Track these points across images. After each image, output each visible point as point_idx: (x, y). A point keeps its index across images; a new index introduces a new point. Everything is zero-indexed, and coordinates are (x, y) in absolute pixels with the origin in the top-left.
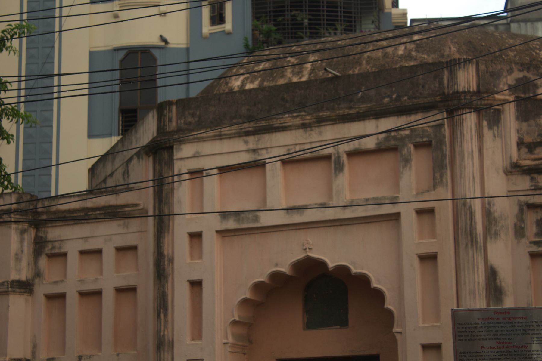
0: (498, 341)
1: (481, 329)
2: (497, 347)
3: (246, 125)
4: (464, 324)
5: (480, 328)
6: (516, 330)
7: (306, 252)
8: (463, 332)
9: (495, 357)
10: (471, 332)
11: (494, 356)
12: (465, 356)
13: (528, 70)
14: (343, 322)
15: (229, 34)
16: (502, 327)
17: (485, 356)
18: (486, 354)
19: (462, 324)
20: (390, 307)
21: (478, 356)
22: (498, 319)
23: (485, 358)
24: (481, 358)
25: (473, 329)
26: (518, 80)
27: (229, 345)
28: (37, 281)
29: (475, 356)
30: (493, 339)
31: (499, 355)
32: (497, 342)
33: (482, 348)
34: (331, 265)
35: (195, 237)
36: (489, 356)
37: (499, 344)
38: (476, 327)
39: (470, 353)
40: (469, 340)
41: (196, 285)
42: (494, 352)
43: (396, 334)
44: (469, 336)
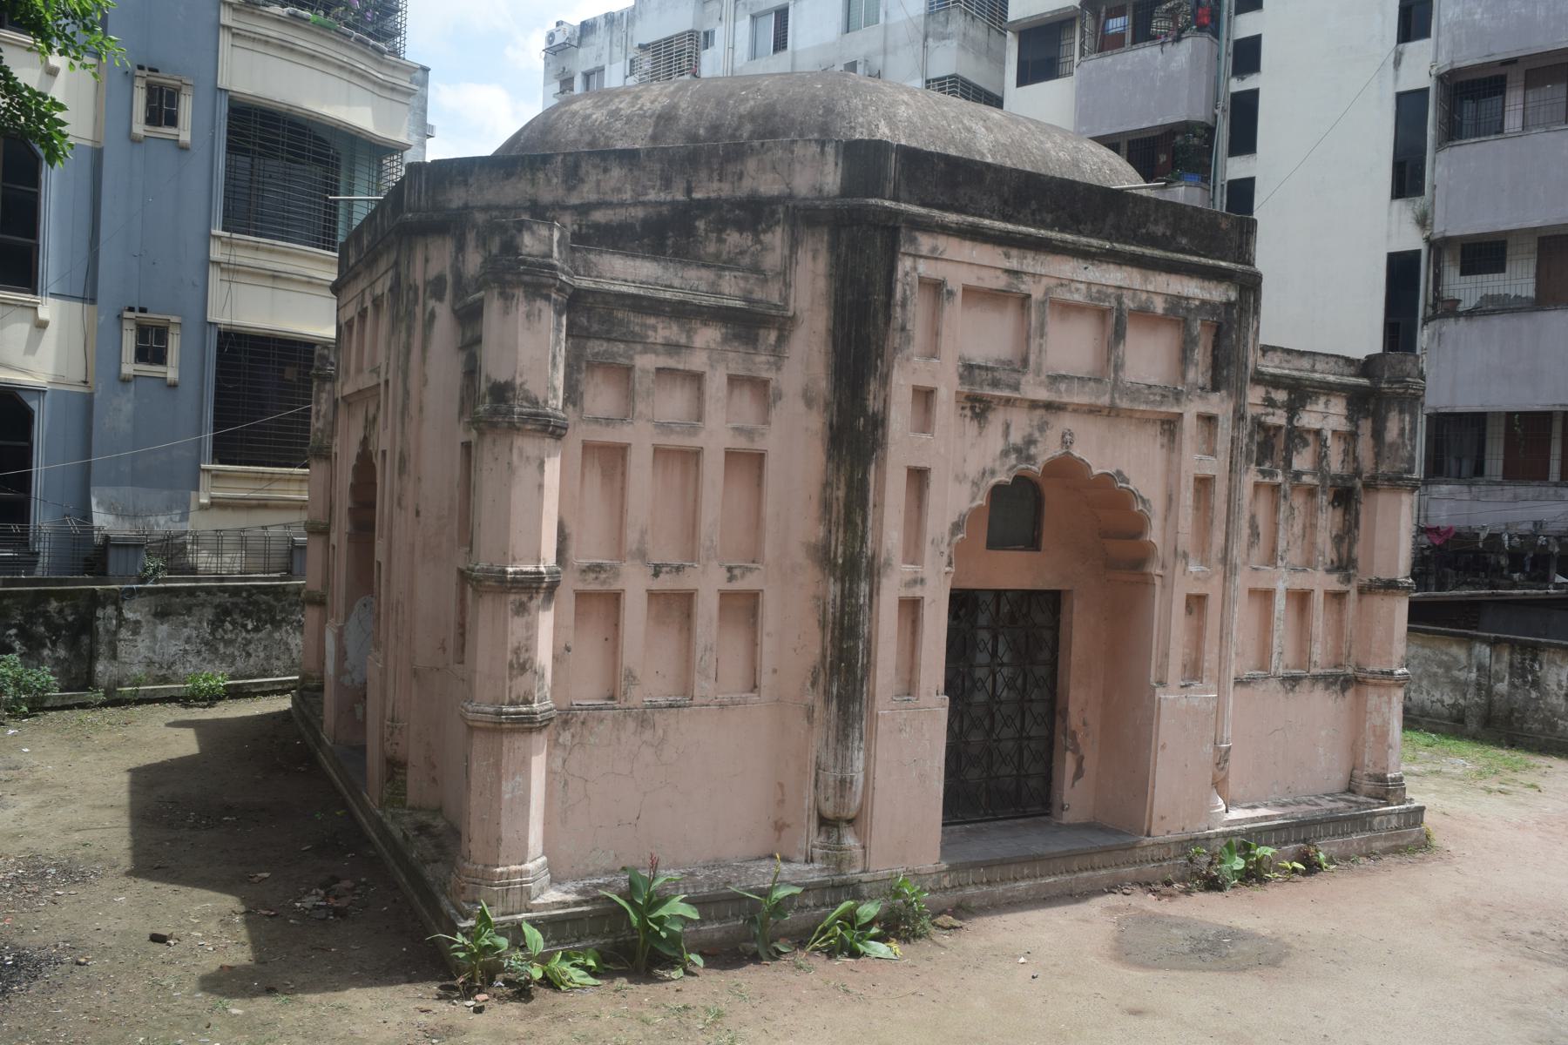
7: (1068, 447)
14: (1033, 543)
20: (1153, 540)
35: (925, 397)
43: (1156, 578)
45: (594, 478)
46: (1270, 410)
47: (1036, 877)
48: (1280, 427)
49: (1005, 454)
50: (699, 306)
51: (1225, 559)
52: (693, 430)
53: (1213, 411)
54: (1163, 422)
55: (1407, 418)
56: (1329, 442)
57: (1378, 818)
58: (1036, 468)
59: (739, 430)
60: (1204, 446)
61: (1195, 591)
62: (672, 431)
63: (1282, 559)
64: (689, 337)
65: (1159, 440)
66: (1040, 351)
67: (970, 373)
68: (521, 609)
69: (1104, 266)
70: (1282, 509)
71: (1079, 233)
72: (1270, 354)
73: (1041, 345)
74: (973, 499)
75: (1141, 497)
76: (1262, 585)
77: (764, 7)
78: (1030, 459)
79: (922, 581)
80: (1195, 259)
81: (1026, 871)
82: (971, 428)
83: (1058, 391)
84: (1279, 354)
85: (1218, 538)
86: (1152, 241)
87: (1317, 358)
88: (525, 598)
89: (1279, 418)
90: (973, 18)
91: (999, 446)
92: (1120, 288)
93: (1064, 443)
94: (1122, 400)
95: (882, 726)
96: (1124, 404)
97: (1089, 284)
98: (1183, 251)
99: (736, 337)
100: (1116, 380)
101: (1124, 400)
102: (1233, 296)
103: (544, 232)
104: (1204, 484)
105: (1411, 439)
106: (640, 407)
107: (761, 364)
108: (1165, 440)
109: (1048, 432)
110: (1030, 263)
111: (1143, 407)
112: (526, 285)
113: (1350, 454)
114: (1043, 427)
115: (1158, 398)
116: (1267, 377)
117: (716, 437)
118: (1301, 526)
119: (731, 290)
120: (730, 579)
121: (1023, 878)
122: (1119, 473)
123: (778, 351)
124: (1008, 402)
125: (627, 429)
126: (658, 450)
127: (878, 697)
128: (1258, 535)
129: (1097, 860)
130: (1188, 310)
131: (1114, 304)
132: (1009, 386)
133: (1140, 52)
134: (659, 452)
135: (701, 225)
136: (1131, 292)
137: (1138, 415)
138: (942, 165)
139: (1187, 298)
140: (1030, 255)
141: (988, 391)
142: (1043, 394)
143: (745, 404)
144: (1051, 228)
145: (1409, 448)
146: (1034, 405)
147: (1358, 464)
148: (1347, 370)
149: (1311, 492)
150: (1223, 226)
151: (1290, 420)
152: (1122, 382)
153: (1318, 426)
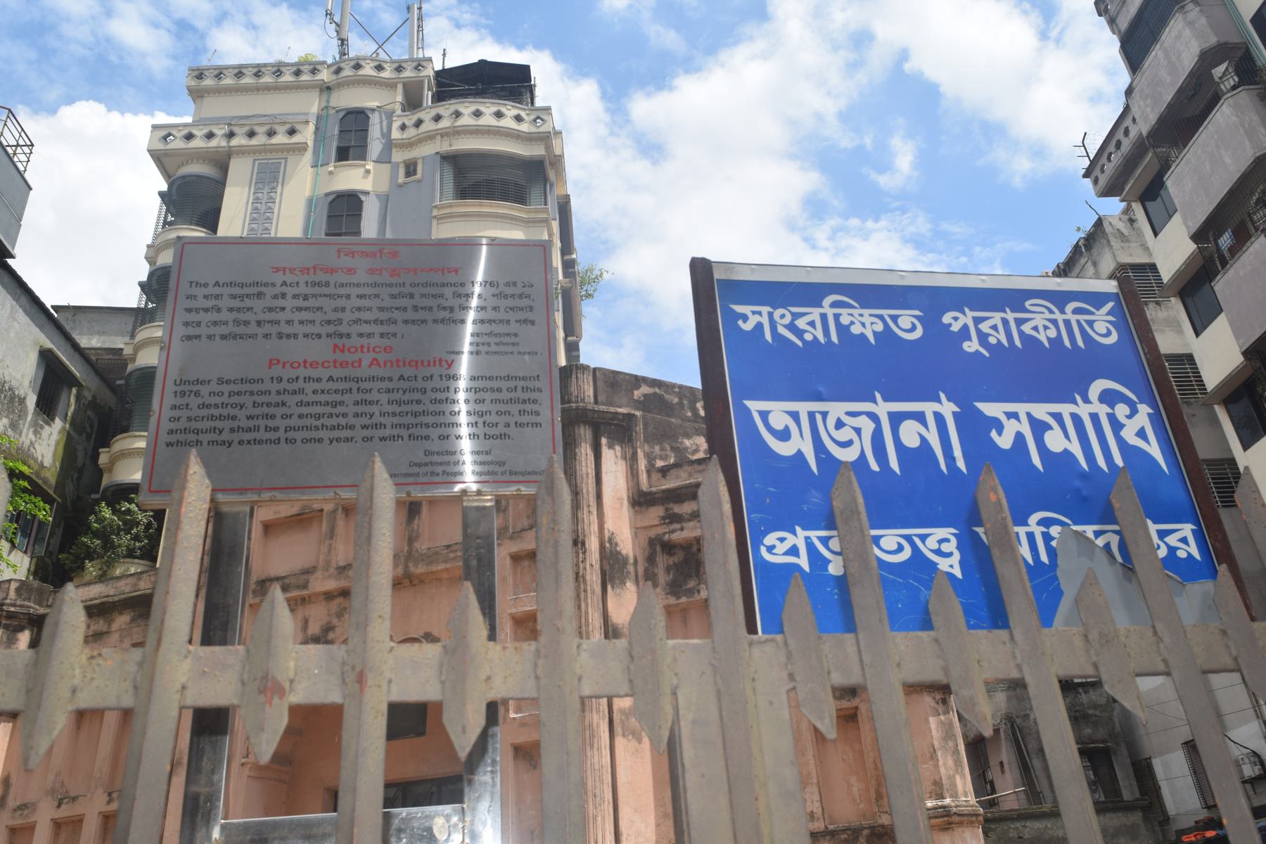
0: (339, 342)
1: (281, 303)
2: (335, 361)
4: (217, 284)
5: (275, 297)
6: (416, 308)
8: (206, 310)
9: (322, 398)
10: (239, 310)
11: (315, 392)
12: (197, 394)
16: (361, 297)
17: (278, 393)
18: (284, 385)
19: (206, 285)
21: (252, 393)
22: (351, 271)
23: (279, 399)
24: (259, 399)
25: (245, 299)
26: (645, 396)
27: (250, 765)
29: (239, 393)
30: (319, 336)
31: (336, 391)
32: (336, 346)
33: (271, 364)
36: (295, 392)
37: (342, 351)
38: (260, 295)
39: (221, 381)
40: (223, 337)
42: (319, 380)
44: (226, 323)
50: (113, 602)
60: (534, 585)
61: (523, 738)
64: (109, 625)
66: (330, 550)
67: (262, 587)
72: (673, 472)
73: (330, 545)
90: (1157, 303)
96: (419, 569)
100: (409, 552)
101: (420, 566)
109: (346, 616)
111: (441, 567)
116: (657, 496)
120: (109, 802)
132: (298, 587)
133: (1251, 249)
137: (445, 575)
142: (332, 585)
146: (329, 596)
152: (417, 551)
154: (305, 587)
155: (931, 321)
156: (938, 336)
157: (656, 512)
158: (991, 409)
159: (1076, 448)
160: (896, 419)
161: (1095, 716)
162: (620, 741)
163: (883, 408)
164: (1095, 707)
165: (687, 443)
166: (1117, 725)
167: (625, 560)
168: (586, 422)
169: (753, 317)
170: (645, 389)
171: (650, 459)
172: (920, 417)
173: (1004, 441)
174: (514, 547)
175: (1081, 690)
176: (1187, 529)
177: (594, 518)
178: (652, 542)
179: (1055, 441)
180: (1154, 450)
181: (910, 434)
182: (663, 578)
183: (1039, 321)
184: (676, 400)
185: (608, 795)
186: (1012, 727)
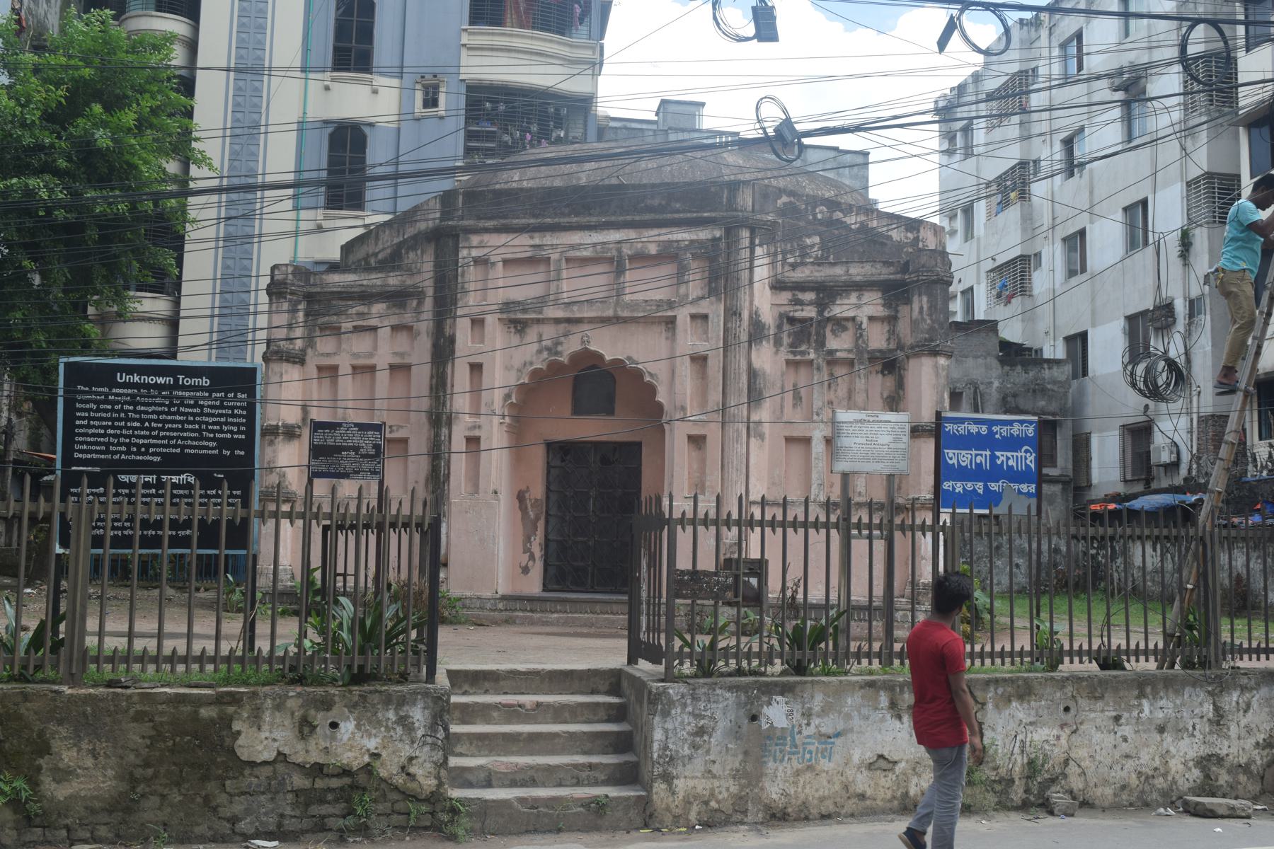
3: (532, 221)
13: (794, 196)
14: (610, 412)
15: (442, 118)
26: (785, 204)
28: (309, 351)
34: (608, 358)
35: (478, 322)
41: (476, 368)
45: (326, 382)
46: (799, 307)
47: (566, 612)
48: (811, 319)
49: (539, 352)
51: (724, 408)
52: (371, 355)
53: (704, 311)
54: (667, 323)
55: (925, 299)
56: (864, 326)
57: (901, 613)
58: (564, 359)
59: (395, 354)
62: (360, 357)
63: (818, 414)
64: (369, 309)
65: (664, 335)
68: (271, 443)
69: (606, 232)
70: (815, 378)
71: (590, 215)
72: (799, 269)
74: (518, 380)
75: (649, 373)
76: (797, 432)
77: (1067, 35)
78: (557, 353)
79: (479, 427)
80: (689, 215)
81: (558, 608)
82: (515, 339)
83: (572, 311)
84: (810, 267)
85: (715, 397)
86: (651, 209)
87: (851, 265)
88: (273, 438)
89: (810, 312)
91: (535, 347)
92: (619, 242)
93: (583, 342)
94: (623, 311)
95: (453, 508)
96: (626, 314)
97: (595, 245)
98: (678, 211)
99: (394, 306)
100: (617, 301)
102: (718, 234)
103: (284, 268)
104: (700, 360)
105: (930, 315)
106: (344, 346)
107: (408, 318)
108: (670, 334)
110: (549, 239)
111: (641, 314)
112: (276, 293)
113: (892, 333)
114: (566, 335)
115: (654, 308)
117: (383, 358)
118: (845, 390)
119: (394, 280)
121: (556, 612)
122: (629, 358)
123: (418, 311)
124: (538, 321)
125: (337, 357)
126: (354, 368)
127: (451, 492)
128: (801, 398)
129: (615, 607)
130: (679, 248)
131: (615, 253)
132: (535, 312)
134: (354, 368)
135: (403, 251)
136: (628, 245)
138: (490, 196)
139: (677, 241)
140: (548, 235)
141: (520, 316)
142: (560, 314)
143: (403, 339)
144: (569, 215)
145: (929, 321)
146: (557, 321)
147: (899, 340)
148: (885, 270)
149: (851, 363)
150: (713, 189)
151: (820, 313)
153: (850, 314)
154: (541, 313)
155: (989, 429)
156: (991, 434)
157: (785, 296)
158: (998, 454)
159: (1015, 465)
160: (976, 455)
161: (1053, 390)
162: (752, 440)
163: (974, 452)
164: (1055, 382)
165: (808, 241)
166: (1070, 401)
167: (764, 325)
168: (746, 227)
169: (949, 427)
170: (785, 199)
171: (784, 253)
172: (981, 455)
173: (999, 462)
174: (694, 310)
175: (1046, 366)
176: (1034, 486)
177: (747, 297)
178: (781, 316)
179: (1011, 463)
180: (1033, 466)
181: (979, 459)
182: (786, 340)
183: (1015, 429)
184: (804, 206)
185: (744, 471)
186: (975, 392)
